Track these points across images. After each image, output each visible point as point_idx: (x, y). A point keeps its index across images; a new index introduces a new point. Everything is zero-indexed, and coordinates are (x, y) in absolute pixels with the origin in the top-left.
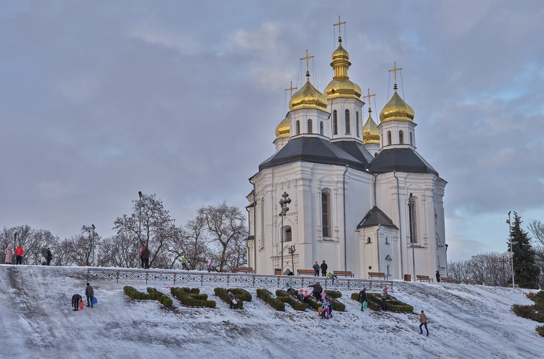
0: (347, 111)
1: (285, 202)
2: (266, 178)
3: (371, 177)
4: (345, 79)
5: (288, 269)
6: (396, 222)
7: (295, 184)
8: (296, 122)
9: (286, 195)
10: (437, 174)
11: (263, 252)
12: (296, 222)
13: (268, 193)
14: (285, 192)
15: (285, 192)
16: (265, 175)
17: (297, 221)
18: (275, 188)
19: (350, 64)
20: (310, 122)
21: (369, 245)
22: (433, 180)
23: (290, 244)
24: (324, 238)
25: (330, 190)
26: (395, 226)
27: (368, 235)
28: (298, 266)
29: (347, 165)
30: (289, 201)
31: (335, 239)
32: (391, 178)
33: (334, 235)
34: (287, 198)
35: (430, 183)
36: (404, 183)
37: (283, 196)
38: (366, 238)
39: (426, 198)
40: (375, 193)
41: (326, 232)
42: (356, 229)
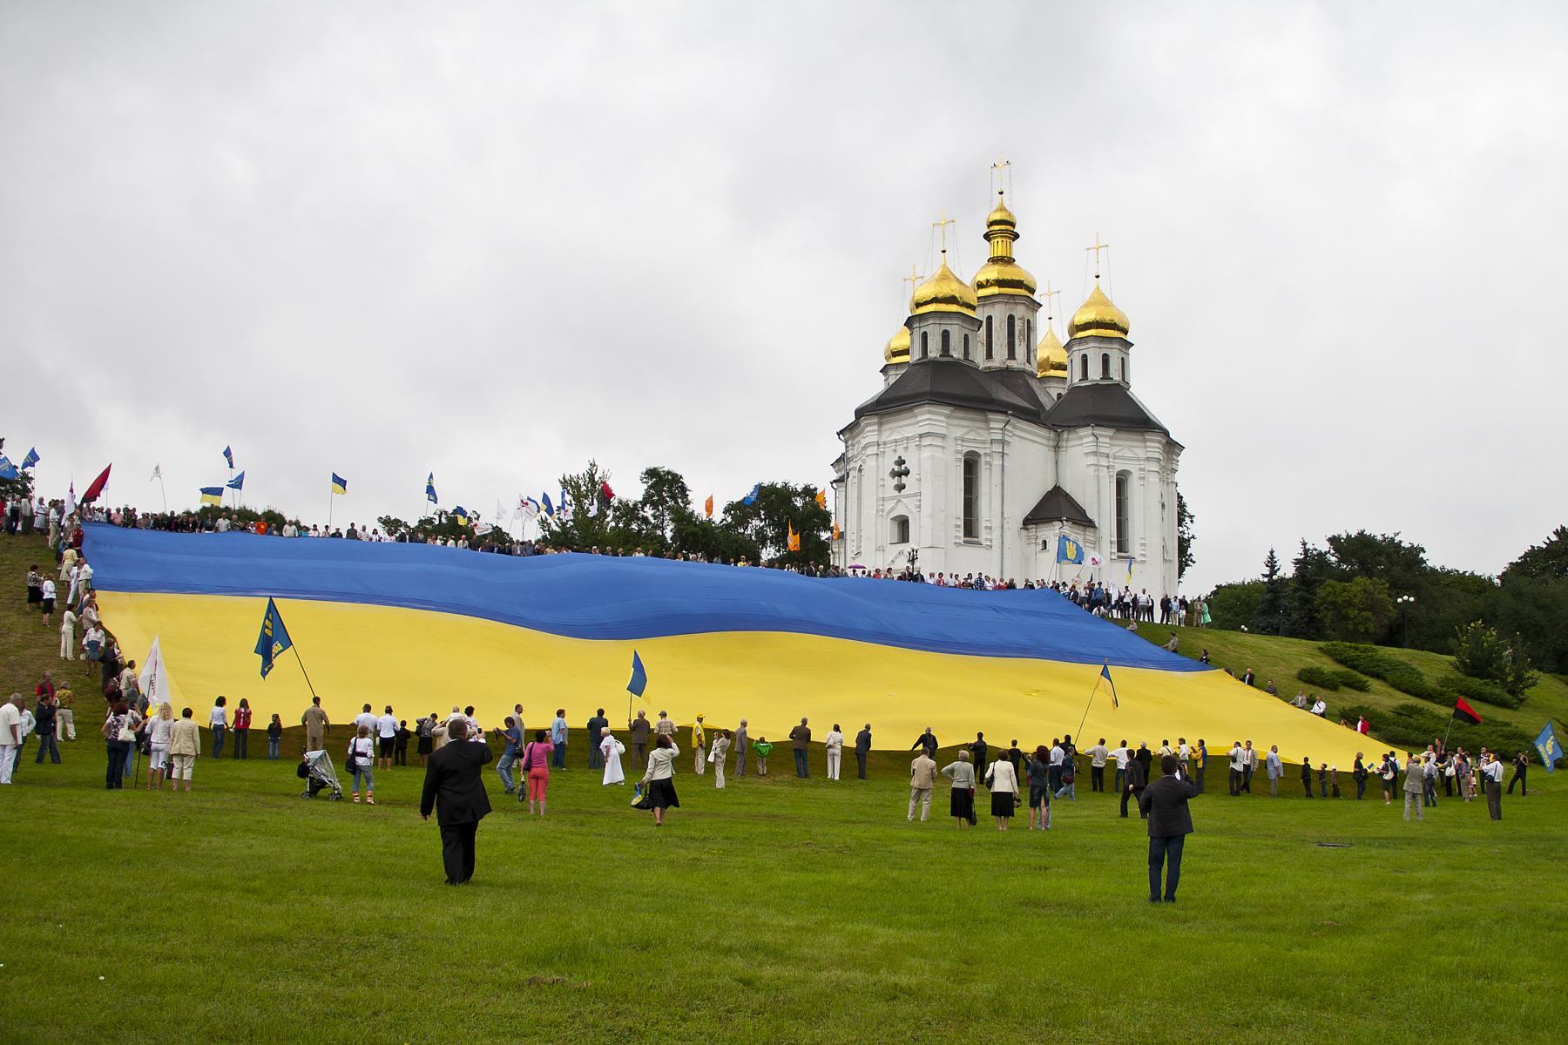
0: (1011, 318)
1: (901, 472)
3: (1052, 435)
4: (1008, 261)
9: (901, 462)
10: (1166, 433)
12: (918, 510)
14: (900, 457)
15: (900, 457)
16: (867, 425)
19: (1017, 236)
20: (946, 335)
22: (1159, 442)
23: (906, 548)
24: (967, 539)
25: (979, 455)
26: (1091, 521)
29: (1010, 412)
30: (907, 473)
32: (1086, 436)
33: (983, 535)
34: (903, 466)
38: (1040, 541)
39: (1146, 474)
40: (1057, 463)
41: (970, 528)
42: (1022, 526)
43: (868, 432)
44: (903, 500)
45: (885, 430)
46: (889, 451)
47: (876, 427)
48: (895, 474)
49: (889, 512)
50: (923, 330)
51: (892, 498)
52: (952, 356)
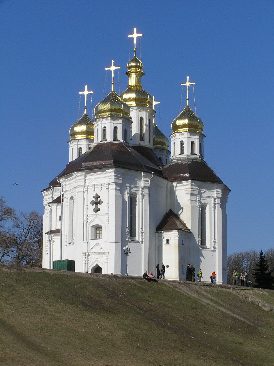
0: (141, 119)
2: (78, 179)
5: (97, 265)
6: (189, 226)
7: (107, 187)
8: (103, 128)
9: (97, 197)
11: (71, 246)
12: (107, 222)
13: (79, 193)
14: (97, 194)
15: (97, 194)
16: (78, 176)
17: (109, 221)
18: (87, 189)
21: (168, 246)
24: (131, 238)
26: (189, 230)
27: (166, 237)
28: (108, 262)
29: (153, 173)
30: (100, 203)
31: (140, 240)
34: (99, 199)
35: (220, 192)
36: (198, 190)
37: (94, 197)
42: (156, 231)
43: (78, 179)
44: (99, 216)
45: (88, 179)
46: (91, 190)
47: (83, 177)
48: (93, 203)
49: (90, 223)
50: (103, 126)
51: (92, 215)
52: (119, 141)
